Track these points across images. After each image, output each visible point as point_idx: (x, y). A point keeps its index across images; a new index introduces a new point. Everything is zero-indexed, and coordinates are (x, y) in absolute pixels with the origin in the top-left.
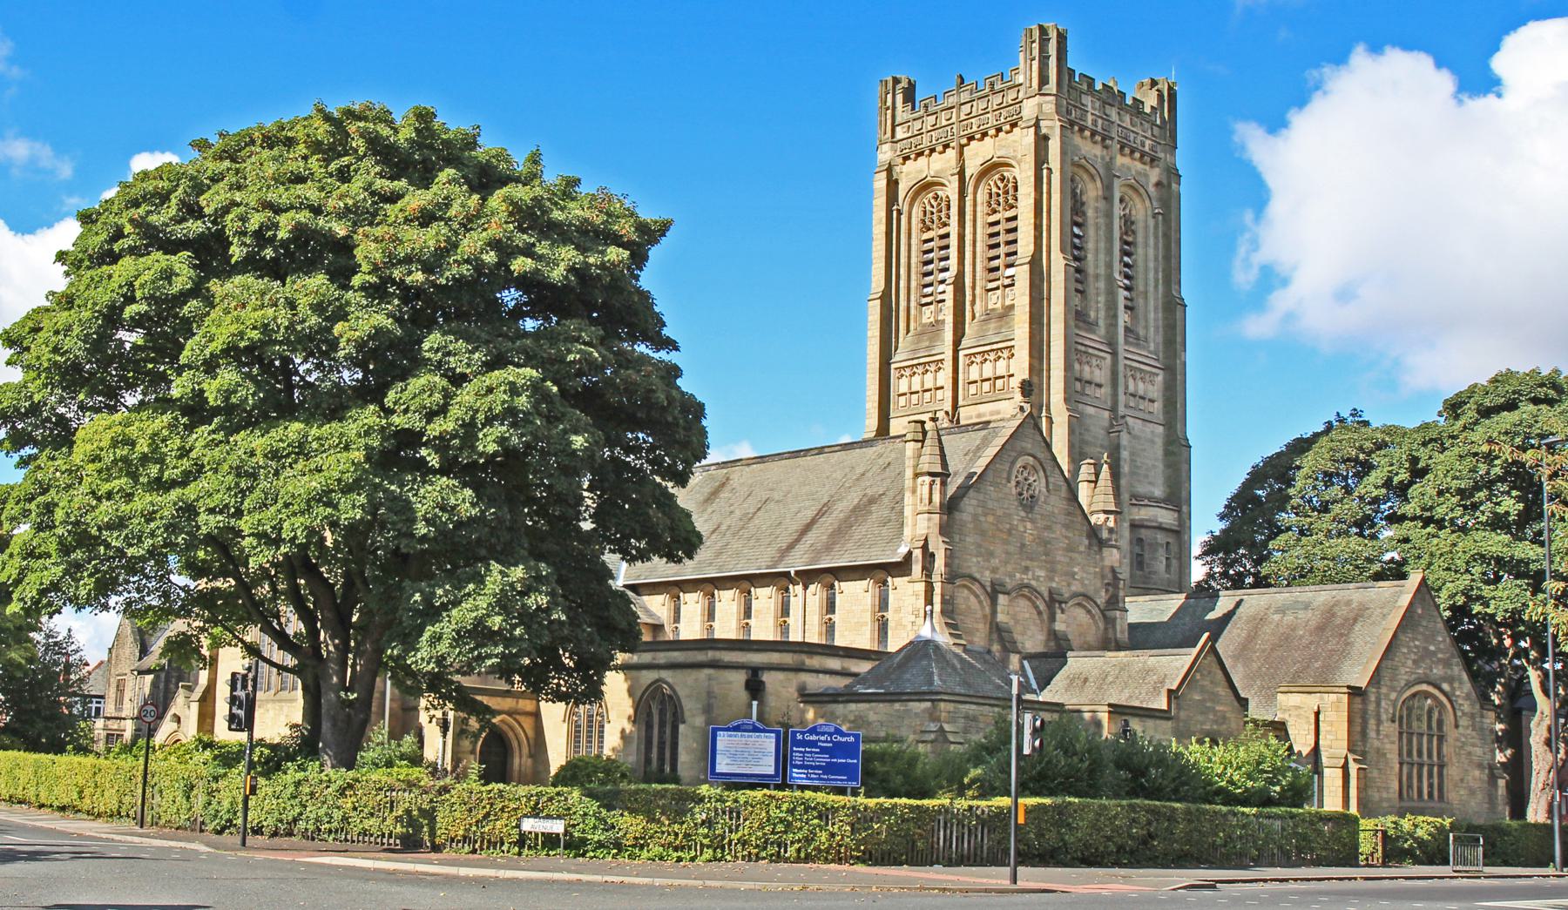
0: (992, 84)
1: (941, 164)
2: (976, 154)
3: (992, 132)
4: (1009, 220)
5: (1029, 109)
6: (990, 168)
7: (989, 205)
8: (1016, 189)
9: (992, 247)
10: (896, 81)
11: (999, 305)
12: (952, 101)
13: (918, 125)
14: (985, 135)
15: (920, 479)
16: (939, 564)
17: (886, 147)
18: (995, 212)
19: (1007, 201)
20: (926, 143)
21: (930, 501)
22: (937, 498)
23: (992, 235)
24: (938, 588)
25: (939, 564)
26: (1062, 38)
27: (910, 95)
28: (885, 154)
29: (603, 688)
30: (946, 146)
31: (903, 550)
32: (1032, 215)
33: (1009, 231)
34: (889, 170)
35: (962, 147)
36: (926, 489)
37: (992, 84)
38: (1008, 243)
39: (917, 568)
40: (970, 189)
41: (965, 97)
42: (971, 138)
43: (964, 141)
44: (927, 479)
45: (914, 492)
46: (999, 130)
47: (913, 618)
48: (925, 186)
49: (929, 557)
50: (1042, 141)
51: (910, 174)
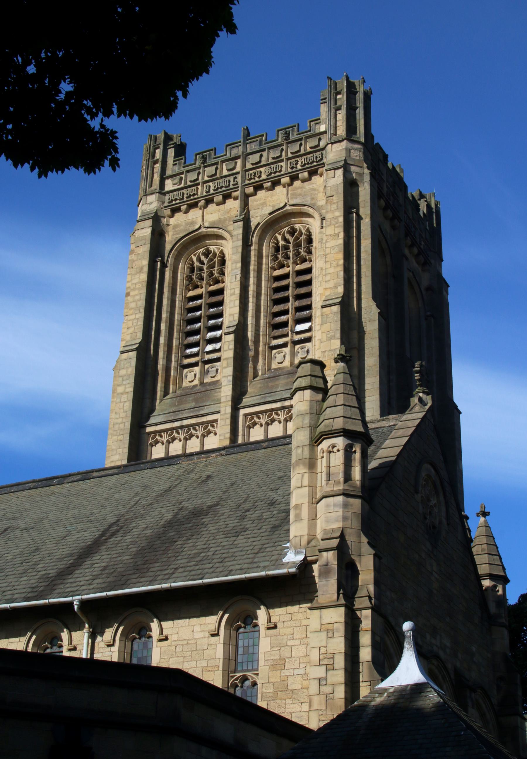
0: (287, 135)
1: (221, 215)
2: (264, 204)
3: (286, 180)
4: (299, 273)
5: (335, 153)
6: (279, 219)
7: (275, 258)
8: (309, 241)
9: (277, 302)
10: (168, 138)
11: (287, 363)
12: (238, 151)
13: (192, 176)
14: (276, 183)
15: (325, 444)
16: (366, 577)
17: (152, 198)
18: (282, 266)
19: (297, 254)
20: (201, 191)
21: (348, 477)
22: (357, 474)
23: (277, 290)
24: (366, 618)
25: (366, 577)
26: (367, 96)
27: (181, 150)
28: (151, 204)
29: (81, 170)
30: (226, 197)
31: (293, 558)
32: (341, 256)
33: (299, 285)
34: (156, 218)
35: (246, 197)
36: (338, 459)
37: (287, 135)
38: (298, 297)
39: (327, 588)
40: (255, 239)
41: (250, 148)
42: (258, 187)
43: (250, 190)
44: (340, 442)
45: (312, 465)
46: (294, 178)
47: (320, 672)
48: (195, 239)
49: (348, 572)
50: (351, 186)
51: (178, 225)
